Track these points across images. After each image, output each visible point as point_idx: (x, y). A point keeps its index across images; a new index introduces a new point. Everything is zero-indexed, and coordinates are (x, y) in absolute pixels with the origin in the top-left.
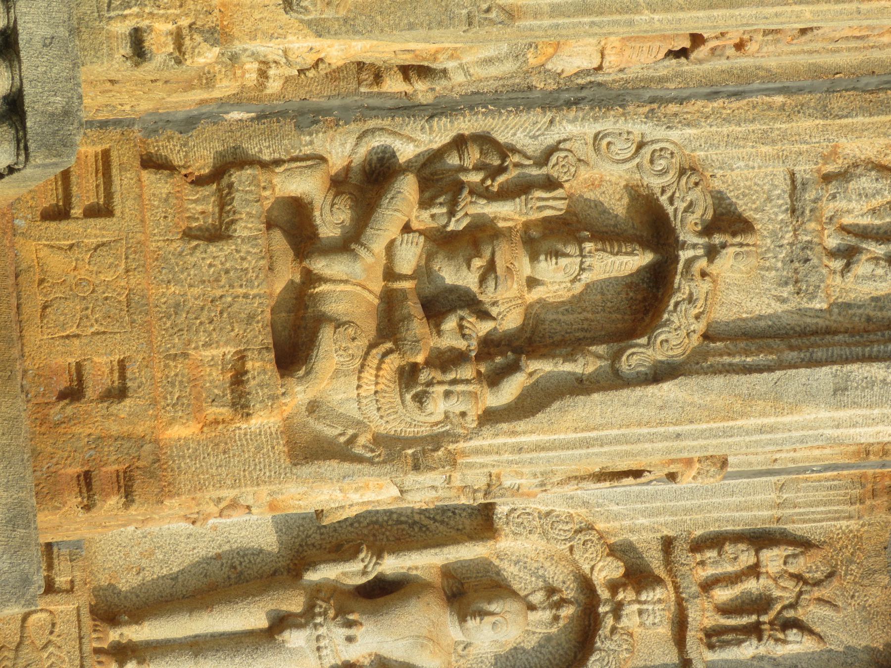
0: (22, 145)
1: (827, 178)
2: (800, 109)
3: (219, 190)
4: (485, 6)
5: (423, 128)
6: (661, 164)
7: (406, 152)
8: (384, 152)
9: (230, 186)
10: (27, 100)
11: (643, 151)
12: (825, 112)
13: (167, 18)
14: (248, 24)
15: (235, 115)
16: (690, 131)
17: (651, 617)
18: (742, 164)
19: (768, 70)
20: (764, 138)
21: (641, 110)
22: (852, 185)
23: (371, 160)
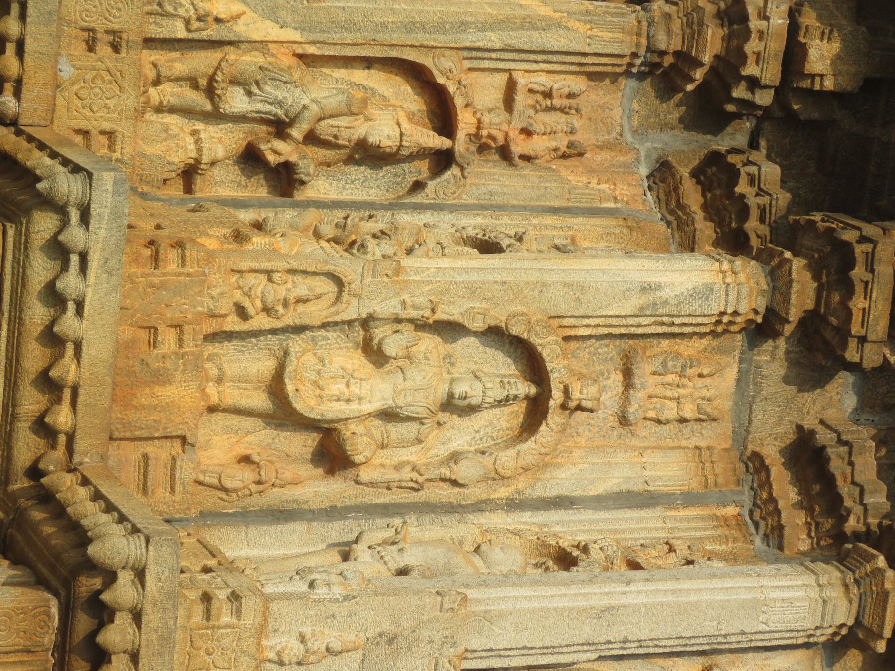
6: (470, 229)
17: (610, 548)
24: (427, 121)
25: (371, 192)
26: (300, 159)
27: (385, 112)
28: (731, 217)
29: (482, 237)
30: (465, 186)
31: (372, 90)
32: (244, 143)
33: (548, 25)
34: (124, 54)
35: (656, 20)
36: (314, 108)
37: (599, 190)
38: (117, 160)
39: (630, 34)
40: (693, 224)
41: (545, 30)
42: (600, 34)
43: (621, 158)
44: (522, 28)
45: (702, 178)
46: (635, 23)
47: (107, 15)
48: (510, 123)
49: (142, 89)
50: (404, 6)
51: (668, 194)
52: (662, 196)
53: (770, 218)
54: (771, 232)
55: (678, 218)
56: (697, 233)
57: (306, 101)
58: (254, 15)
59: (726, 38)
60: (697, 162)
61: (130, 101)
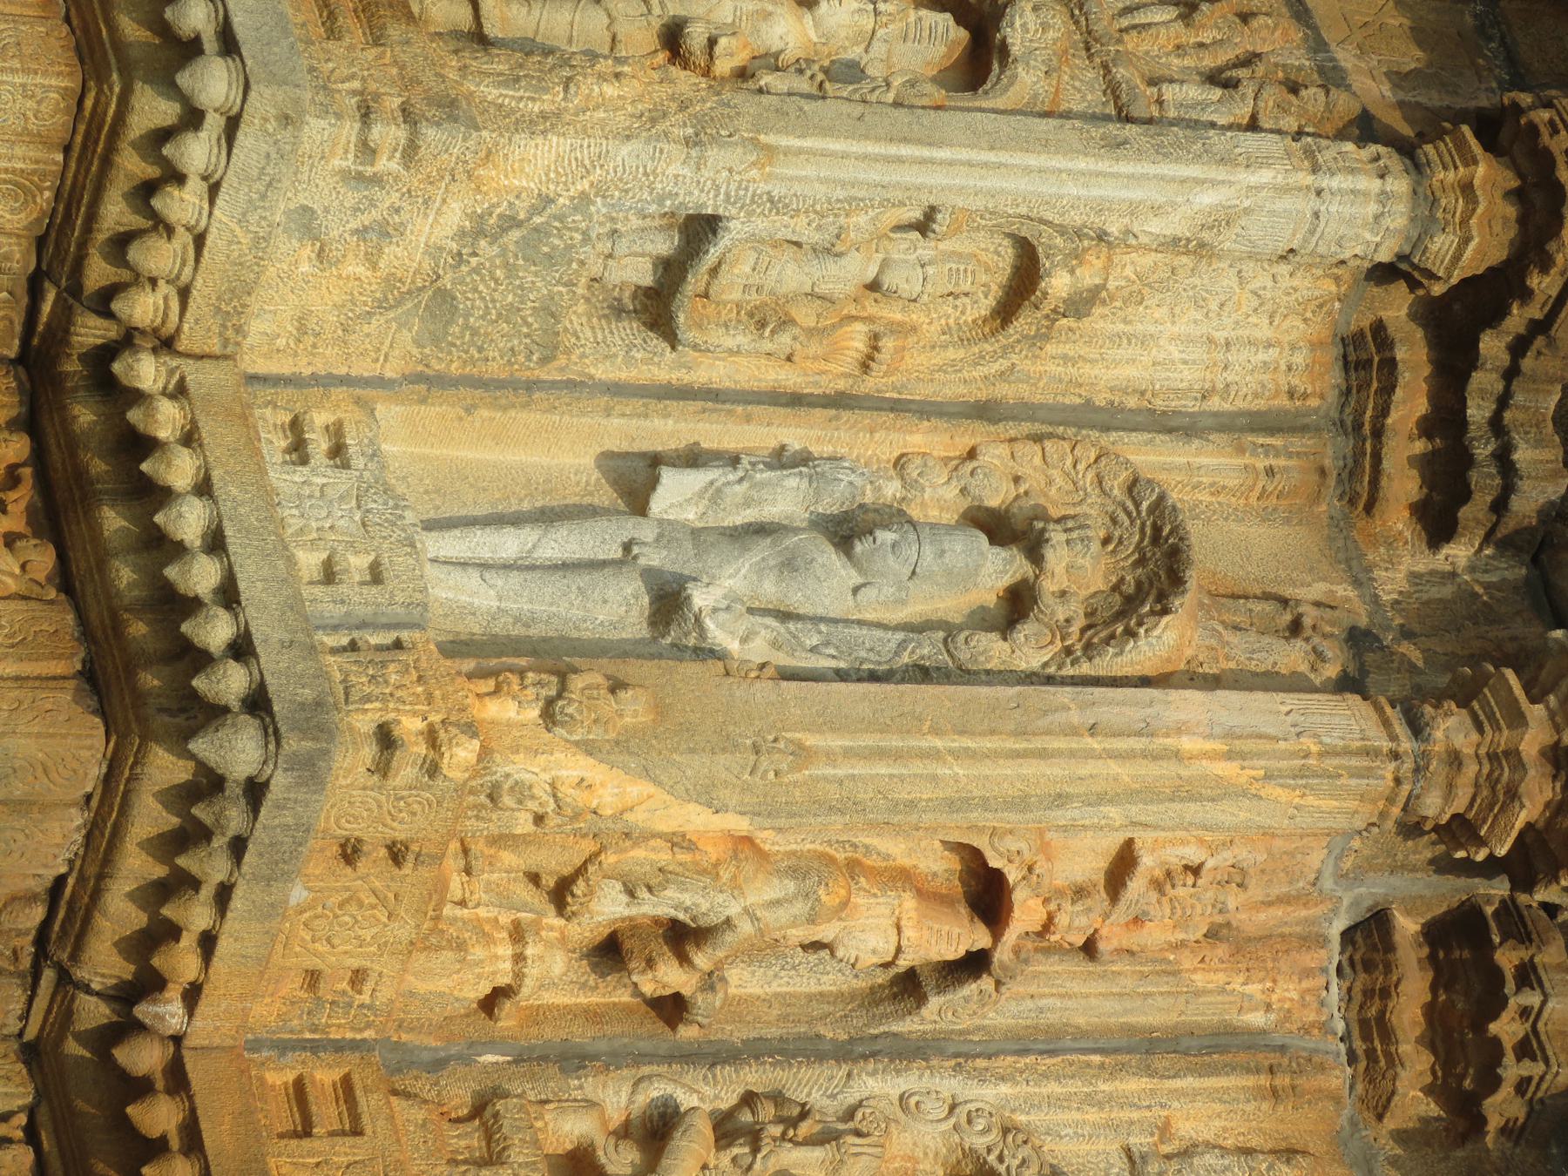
0: (270, 730)
1: (1168, 1157)
2: (1122, 1067)
3: (484, 1124)
4: (771, 738)
5: (705, 1077)
6: (980, 1124)
7: (686, 1100)
8: (665, 1105)
9: (496, 1115)
10: (271, 689)
11: (957, 1111)
12: (1151, 1072)
13: (415, 714)
14: (508, 741)
15: (489, 1058)
16: (1005, 1089)
18: (1070, 1131)
19: (1078, 1028)
20: (1090, 1100)
21: (947, 1064)
22: (1196, 1161)
23: (651, 1115)
24: (957, 882)
25: (824, 978)
26: (702, 989)
27: (881, 900)
28: (1466, 1069)
29: (995, 1164)
30: (996, 1002)
31: (866, 847)
32: (607, 931)
33: (1224, 791)
34: (408, 868)
35: (1431, 768)
36: (746, 928)
37: (1243, 994)
38: (362, 1006)
39: (1374, 801)
40: (1394, 1080)
41: (1213, 800)
42: (1316, 803)
43: (1304, 913)
44: (1172, 800)
45: (1441, 955)
46: (1390, 776)
47: (389, 821)
48: (1106, 916)
49: (431, 913)
50: (956, 769)
51: (1368, 994)
52: (1358, 997)
53: (1535, 1093)
54: (1529, 1115)
55: (1371, 1055)
56: (1396, 1098)
57: (734, 910)
58: (668, 798)
59: (1553, 805)
60: (1444, 909)
61: (403, 930)
